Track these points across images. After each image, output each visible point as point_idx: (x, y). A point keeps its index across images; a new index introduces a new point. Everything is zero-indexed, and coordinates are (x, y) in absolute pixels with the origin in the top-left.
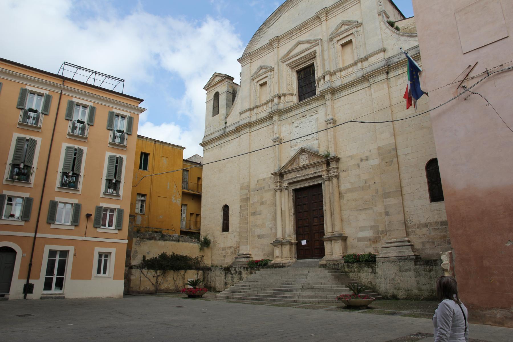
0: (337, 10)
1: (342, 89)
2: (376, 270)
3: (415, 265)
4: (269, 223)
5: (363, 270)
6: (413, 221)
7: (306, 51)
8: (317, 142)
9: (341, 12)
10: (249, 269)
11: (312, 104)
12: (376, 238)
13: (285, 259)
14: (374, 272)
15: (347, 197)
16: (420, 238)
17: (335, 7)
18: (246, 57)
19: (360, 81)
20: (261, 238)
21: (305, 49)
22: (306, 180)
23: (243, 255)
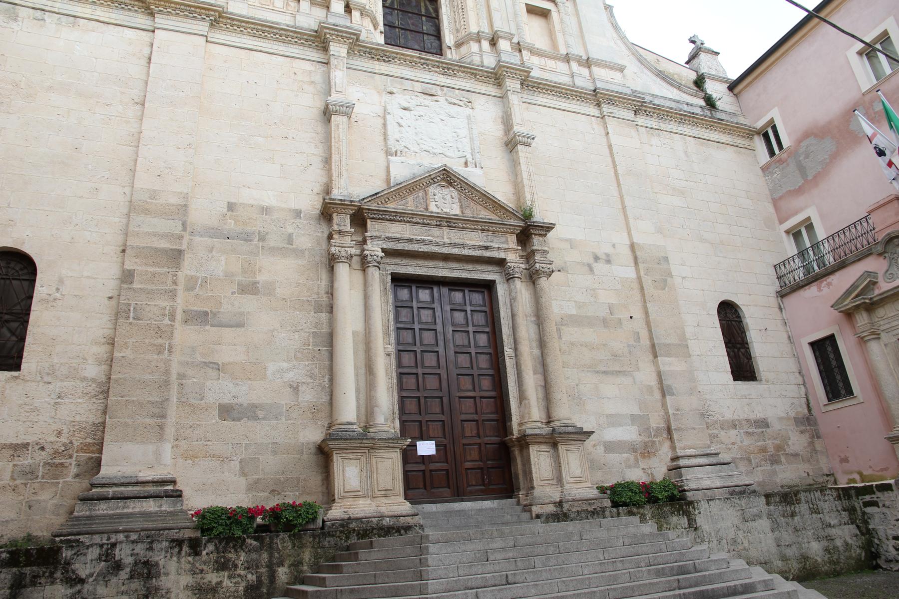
1: (542, 89)
2: (697, 521)
3: (768, 504)
4: (285, 365)
5: (668, 524)
6: (711, 413)
8: (478, 171)
10: (211, 547)
12: (646, 445)
13: (384, 500)
14: (692, 525)
15: (571, 334)
16: (727, 449)
19: (583, 95)
20: (239, 419)
22: (446, 258)
23: (137, 483)
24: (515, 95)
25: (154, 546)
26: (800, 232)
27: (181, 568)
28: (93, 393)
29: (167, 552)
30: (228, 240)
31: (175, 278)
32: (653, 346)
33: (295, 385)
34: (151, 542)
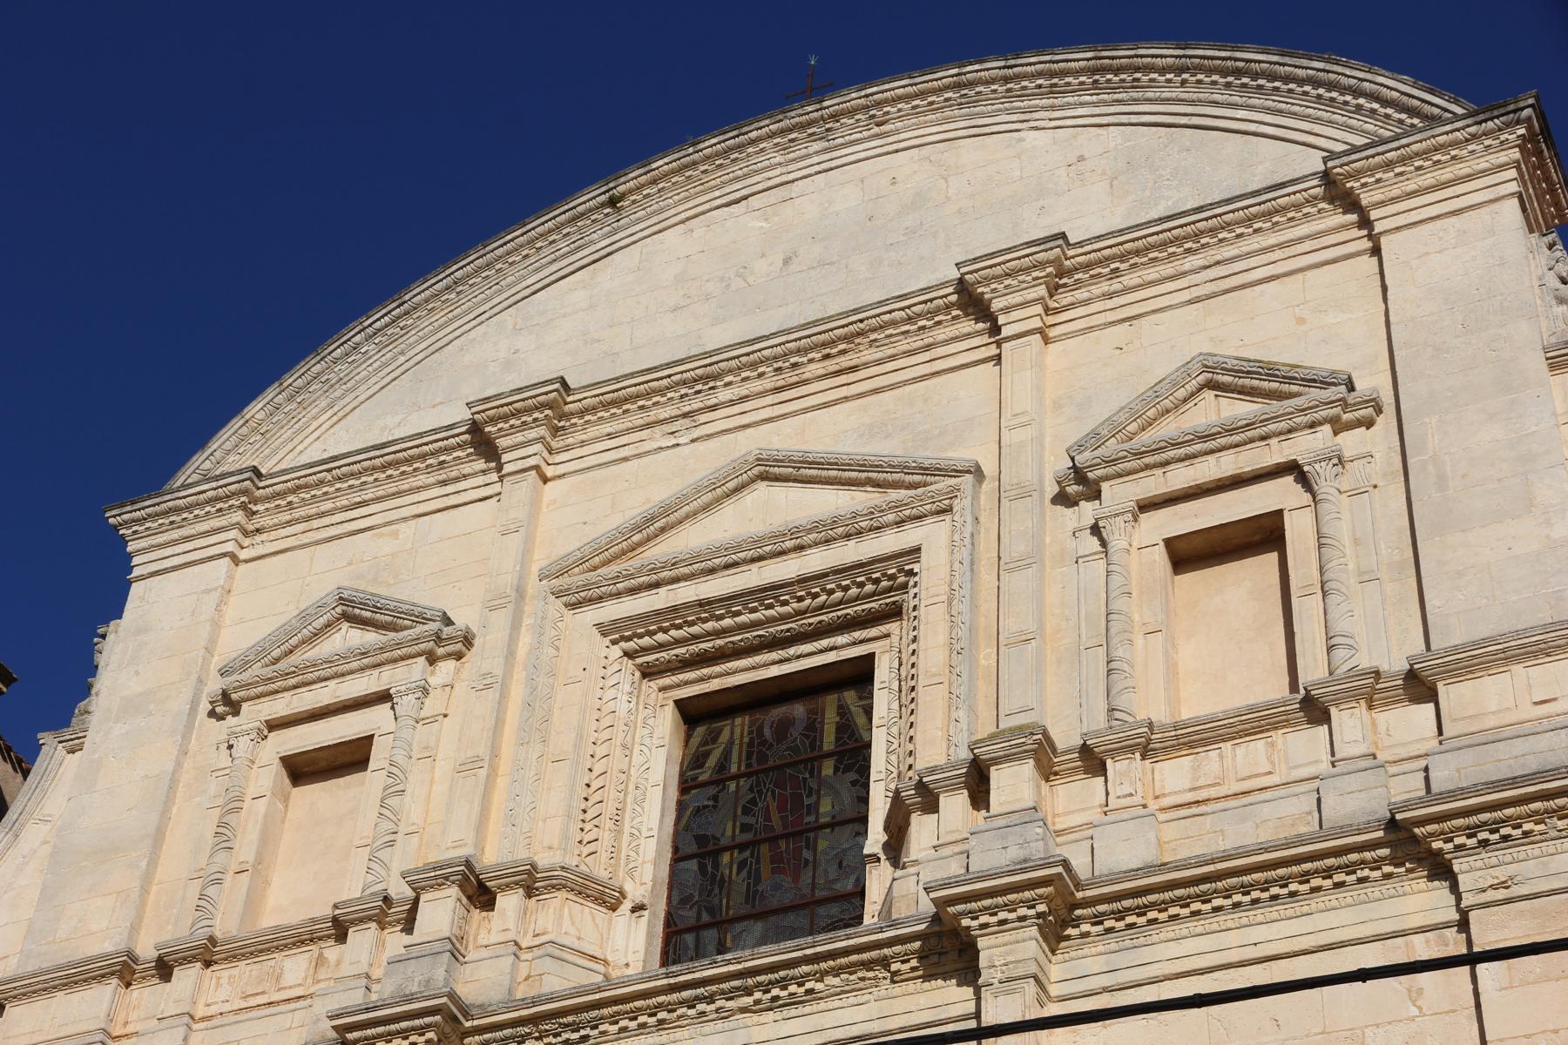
0: (1151, 274)
1: (1162, 906)
7: (816, 544)
9: (1190, 302)
11: (822, 1005)
17: (1137, 253)
18: (209, 502)
21: (816, 526)
24: (1013, 992)
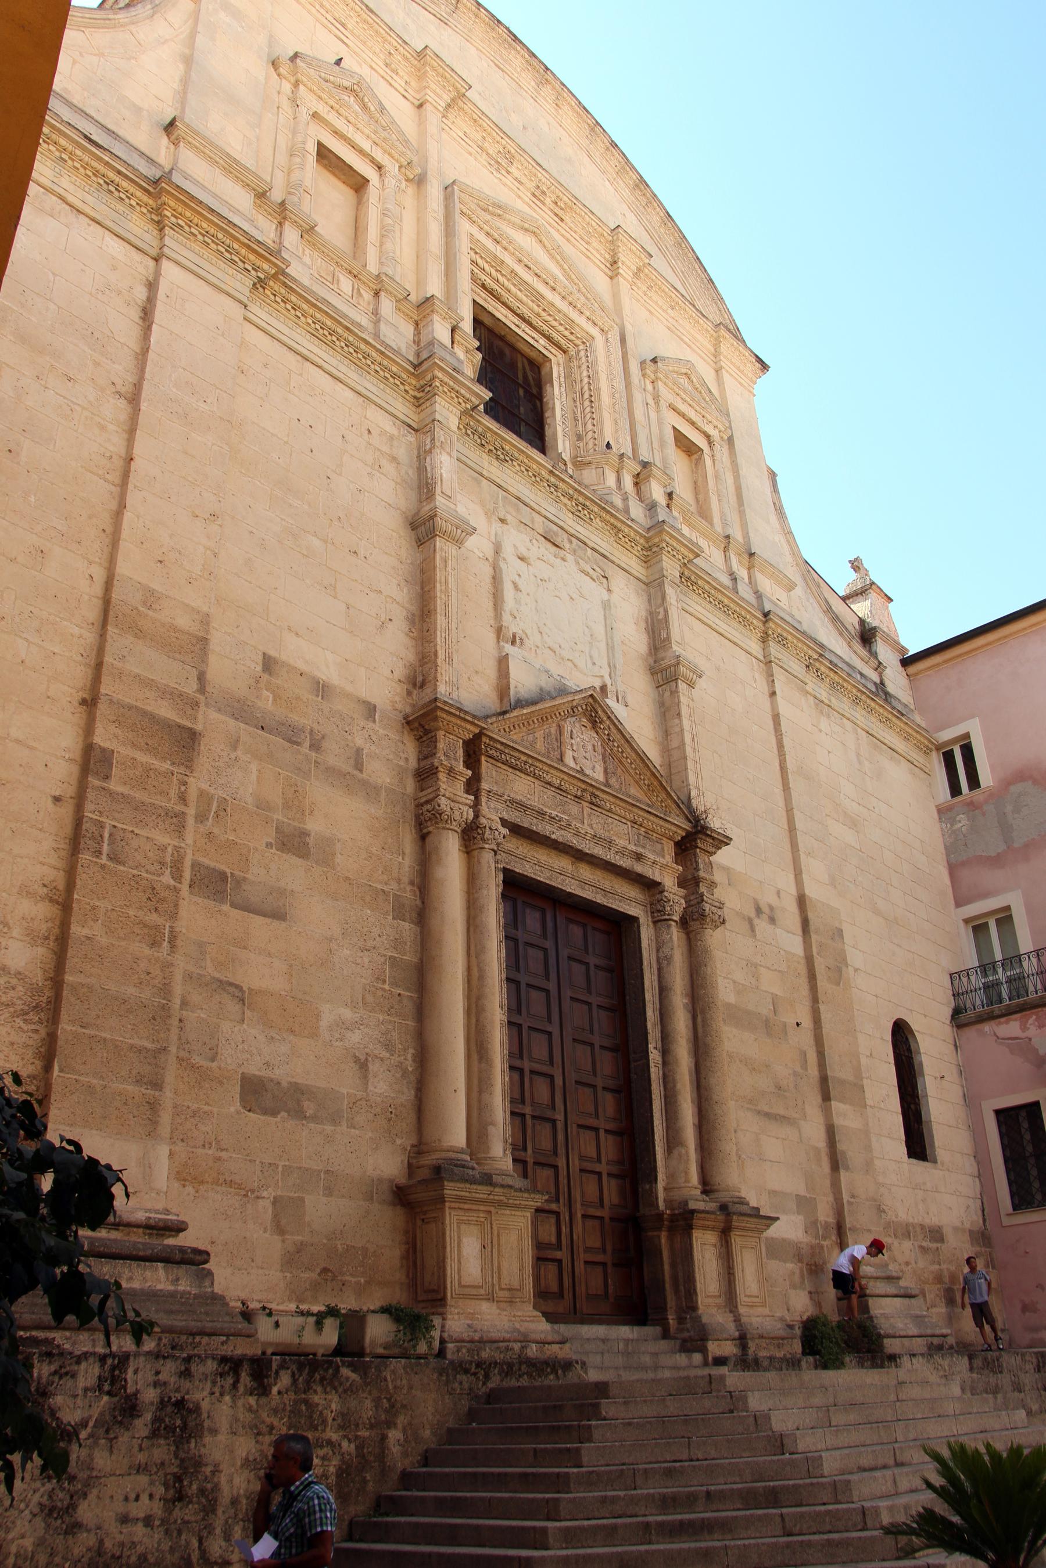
4: (347, 1014)
10: (285, 1379)
20: (274, 1113)
25: (193, 1368)
26: (986, 925)
27: (237, 1420)
28: (19, 1006)
29: (214, 1383)
30: (260, 732)
31: (183, 788)
32: (824, 1080)
33: (362, 1058)
34: (188, 1360)
